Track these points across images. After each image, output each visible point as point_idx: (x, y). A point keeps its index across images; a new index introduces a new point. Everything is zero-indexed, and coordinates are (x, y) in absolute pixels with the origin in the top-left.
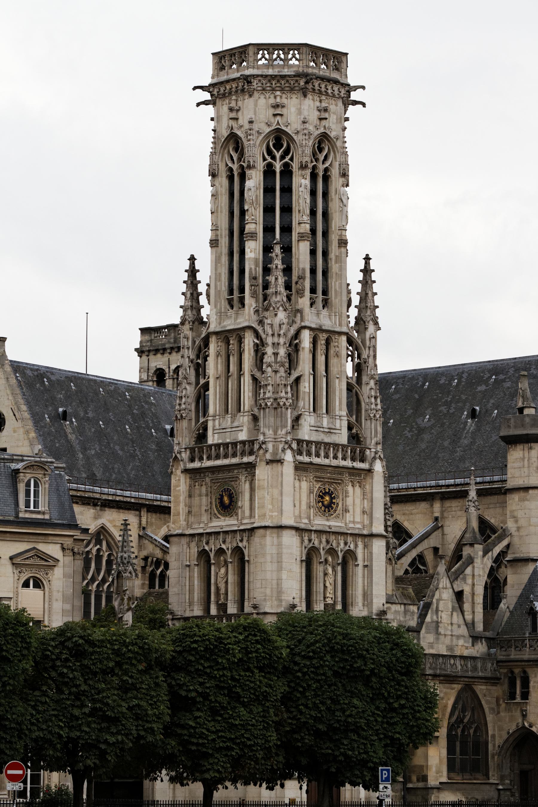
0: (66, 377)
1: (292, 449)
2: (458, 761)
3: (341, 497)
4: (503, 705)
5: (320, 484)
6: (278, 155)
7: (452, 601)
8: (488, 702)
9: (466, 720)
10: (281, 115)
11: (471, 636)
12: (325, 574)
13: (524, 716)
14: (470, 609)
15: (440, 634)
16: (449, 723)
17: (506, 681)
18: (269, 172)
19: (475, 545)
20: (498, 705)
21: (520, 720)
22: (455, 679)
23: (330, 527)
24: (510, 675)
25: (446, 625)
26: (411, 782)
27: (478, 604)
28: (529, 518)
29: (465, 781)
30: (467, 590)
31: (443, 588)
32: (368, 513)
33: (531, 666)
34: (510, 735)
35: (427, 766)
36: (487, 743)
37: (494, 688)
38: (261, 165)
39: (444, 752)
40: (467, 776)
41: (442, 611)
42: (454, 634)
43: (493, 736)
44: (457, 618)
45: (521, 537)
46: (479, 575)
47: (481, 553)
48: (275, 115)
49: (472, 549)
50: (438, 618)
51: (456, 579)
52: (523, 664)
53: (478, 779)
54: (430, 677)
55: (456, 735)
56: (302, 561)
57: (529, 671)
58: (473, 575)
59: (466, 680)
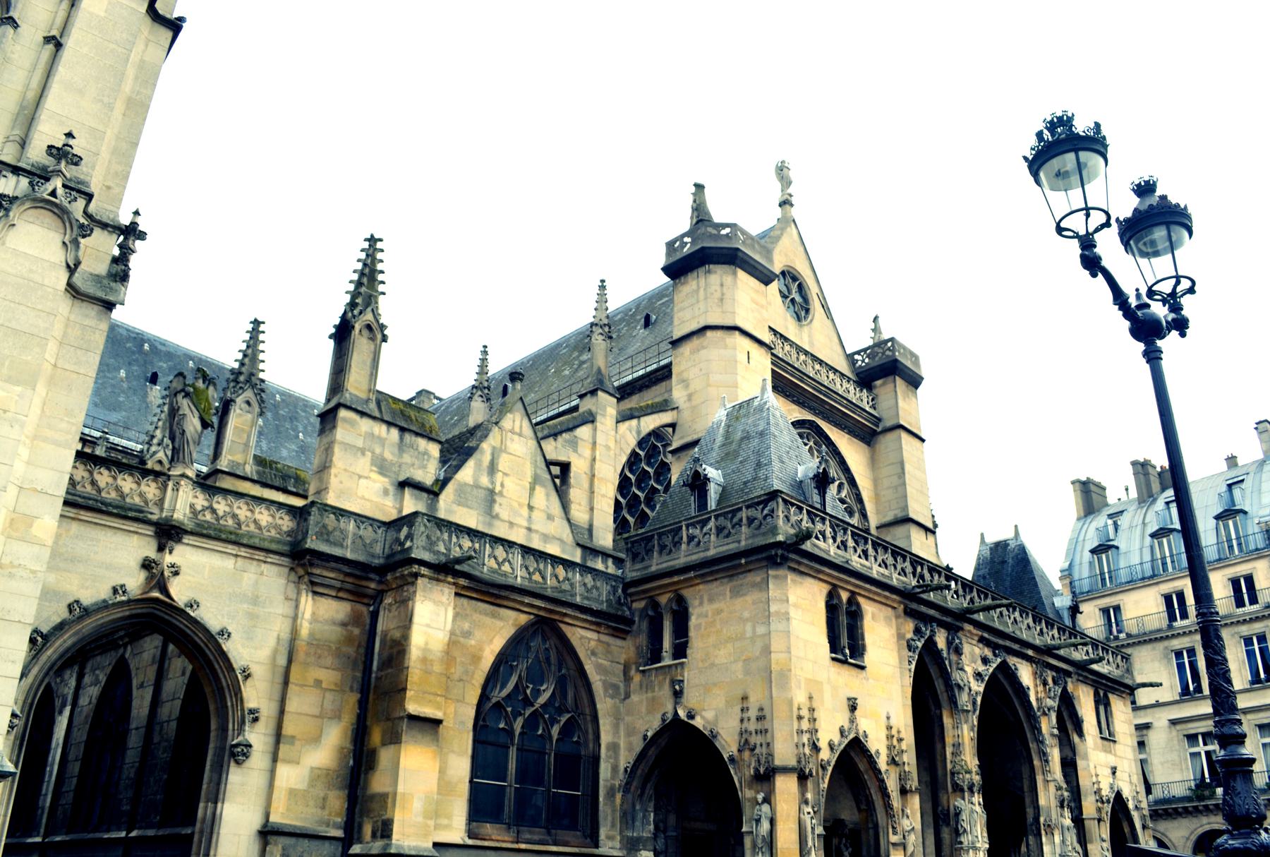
0: (185, 354)
2: (510, 795)
4: (637, 678)
7: (535, 463)
8: (600, 669)
9: (542, 699)
11: (578, 545)
13: (678, 695)
14: (585, 502)
15: (497, 517)
16: (484, 698)
17: (645, 625)
19: (600, 393)
20: (627, 678)
21: (669, 707)
22: (503, 593)
24: (650, 613)
25: (515, 505)
26: (360, 841)
27: (603, 496)
28: (707, 375)
29: (523, 846)
30: (579, 467)
31: (512, 432)
33: (689, 583)
34: (650, 743)
35: (395, 794)
36: (596, 760)
37: (619, 642)
39: (461, 767)
40: (538, 834)
41: (505, 474)
42: (533, 527)
43: (614, 747)
44: (545, 498)
45: (694, 408)
46: (608, 448)
49: (594, 399)
50: (493, 483)
51: (555, 435)
52: (676, 579)
53: (566, 844)
54: (424, 570)
55: (509, 732)
57: (686, 593)
58: (594, 443)
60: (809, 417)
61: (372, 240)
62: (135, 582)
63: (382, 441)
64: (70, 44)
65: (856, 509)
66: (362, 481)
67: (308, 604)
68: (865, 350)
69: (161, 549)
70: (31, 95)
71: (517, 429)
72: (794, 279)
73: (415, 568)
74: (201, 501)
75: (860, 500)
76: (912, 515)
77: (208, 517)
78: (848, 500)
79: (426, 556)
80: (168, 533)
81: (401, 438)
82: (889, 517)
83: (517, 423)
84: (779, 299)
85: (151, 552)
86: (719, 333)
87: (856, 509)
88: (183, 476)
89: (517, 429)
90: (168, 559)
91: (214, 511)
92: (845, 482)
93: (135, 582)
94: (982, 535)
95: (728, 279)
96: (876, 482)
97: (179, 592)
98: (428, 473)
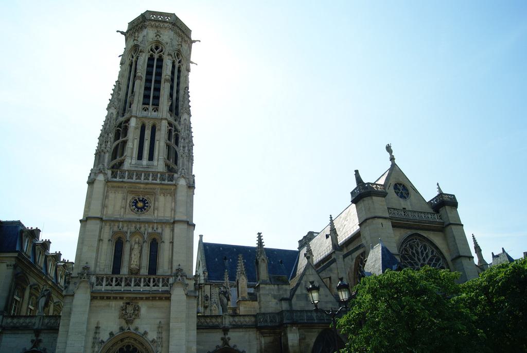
1: (105, 174)
3: (153, 202)
5: (133, 196)
6: (134, 56)
10: (137, 40)
12: (131, 249)
18: (131, 66)
19: (336, 252)
23: (139, 219)
31: (310, 275)
32: (174, 210)
38: (128, 62)
47: (342, 256)
48: (134, 40)
56: (109, 240)
59: (323, 325)
60: (414, 231)
61: (259, 234)
62: (220, 343)
63: (273, 290)
64: (174, 243)
65: (440, 257)
66: (270, 303)
67: (263, 340)
68: (434, 199)
69: (225, 334)
70: (170, 257)
71: (311, 273)
72: (400, 184)
73: (285, 325)
74: (231, 319)
75: (441, 253)
76: (461, 254)
77: (234, 323)
78: (437, 255)
79: (288, 321)
80: (226, 330)
81: (278, 287)
82: (454, 256)
83: (311, 271)
84: (395, 194)
85: (223, 336)
86: (371, 220)
87: (440, 257)
88: (226, 315)
89: (311, 273)
90: (227, 336)
91: (235, 321)
92: (434, 249)
93: (220, 343)
94: (492, 253)
95: (370, 202)
96: (448, 245)
97: (231, 343)
98: (288, 295)
